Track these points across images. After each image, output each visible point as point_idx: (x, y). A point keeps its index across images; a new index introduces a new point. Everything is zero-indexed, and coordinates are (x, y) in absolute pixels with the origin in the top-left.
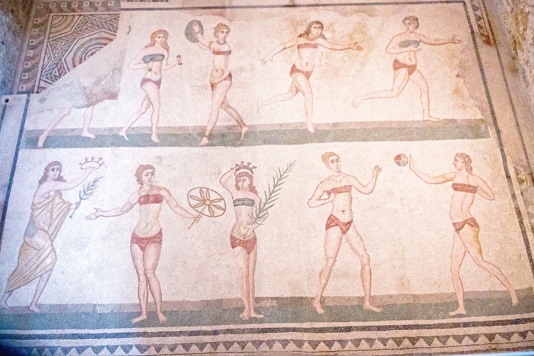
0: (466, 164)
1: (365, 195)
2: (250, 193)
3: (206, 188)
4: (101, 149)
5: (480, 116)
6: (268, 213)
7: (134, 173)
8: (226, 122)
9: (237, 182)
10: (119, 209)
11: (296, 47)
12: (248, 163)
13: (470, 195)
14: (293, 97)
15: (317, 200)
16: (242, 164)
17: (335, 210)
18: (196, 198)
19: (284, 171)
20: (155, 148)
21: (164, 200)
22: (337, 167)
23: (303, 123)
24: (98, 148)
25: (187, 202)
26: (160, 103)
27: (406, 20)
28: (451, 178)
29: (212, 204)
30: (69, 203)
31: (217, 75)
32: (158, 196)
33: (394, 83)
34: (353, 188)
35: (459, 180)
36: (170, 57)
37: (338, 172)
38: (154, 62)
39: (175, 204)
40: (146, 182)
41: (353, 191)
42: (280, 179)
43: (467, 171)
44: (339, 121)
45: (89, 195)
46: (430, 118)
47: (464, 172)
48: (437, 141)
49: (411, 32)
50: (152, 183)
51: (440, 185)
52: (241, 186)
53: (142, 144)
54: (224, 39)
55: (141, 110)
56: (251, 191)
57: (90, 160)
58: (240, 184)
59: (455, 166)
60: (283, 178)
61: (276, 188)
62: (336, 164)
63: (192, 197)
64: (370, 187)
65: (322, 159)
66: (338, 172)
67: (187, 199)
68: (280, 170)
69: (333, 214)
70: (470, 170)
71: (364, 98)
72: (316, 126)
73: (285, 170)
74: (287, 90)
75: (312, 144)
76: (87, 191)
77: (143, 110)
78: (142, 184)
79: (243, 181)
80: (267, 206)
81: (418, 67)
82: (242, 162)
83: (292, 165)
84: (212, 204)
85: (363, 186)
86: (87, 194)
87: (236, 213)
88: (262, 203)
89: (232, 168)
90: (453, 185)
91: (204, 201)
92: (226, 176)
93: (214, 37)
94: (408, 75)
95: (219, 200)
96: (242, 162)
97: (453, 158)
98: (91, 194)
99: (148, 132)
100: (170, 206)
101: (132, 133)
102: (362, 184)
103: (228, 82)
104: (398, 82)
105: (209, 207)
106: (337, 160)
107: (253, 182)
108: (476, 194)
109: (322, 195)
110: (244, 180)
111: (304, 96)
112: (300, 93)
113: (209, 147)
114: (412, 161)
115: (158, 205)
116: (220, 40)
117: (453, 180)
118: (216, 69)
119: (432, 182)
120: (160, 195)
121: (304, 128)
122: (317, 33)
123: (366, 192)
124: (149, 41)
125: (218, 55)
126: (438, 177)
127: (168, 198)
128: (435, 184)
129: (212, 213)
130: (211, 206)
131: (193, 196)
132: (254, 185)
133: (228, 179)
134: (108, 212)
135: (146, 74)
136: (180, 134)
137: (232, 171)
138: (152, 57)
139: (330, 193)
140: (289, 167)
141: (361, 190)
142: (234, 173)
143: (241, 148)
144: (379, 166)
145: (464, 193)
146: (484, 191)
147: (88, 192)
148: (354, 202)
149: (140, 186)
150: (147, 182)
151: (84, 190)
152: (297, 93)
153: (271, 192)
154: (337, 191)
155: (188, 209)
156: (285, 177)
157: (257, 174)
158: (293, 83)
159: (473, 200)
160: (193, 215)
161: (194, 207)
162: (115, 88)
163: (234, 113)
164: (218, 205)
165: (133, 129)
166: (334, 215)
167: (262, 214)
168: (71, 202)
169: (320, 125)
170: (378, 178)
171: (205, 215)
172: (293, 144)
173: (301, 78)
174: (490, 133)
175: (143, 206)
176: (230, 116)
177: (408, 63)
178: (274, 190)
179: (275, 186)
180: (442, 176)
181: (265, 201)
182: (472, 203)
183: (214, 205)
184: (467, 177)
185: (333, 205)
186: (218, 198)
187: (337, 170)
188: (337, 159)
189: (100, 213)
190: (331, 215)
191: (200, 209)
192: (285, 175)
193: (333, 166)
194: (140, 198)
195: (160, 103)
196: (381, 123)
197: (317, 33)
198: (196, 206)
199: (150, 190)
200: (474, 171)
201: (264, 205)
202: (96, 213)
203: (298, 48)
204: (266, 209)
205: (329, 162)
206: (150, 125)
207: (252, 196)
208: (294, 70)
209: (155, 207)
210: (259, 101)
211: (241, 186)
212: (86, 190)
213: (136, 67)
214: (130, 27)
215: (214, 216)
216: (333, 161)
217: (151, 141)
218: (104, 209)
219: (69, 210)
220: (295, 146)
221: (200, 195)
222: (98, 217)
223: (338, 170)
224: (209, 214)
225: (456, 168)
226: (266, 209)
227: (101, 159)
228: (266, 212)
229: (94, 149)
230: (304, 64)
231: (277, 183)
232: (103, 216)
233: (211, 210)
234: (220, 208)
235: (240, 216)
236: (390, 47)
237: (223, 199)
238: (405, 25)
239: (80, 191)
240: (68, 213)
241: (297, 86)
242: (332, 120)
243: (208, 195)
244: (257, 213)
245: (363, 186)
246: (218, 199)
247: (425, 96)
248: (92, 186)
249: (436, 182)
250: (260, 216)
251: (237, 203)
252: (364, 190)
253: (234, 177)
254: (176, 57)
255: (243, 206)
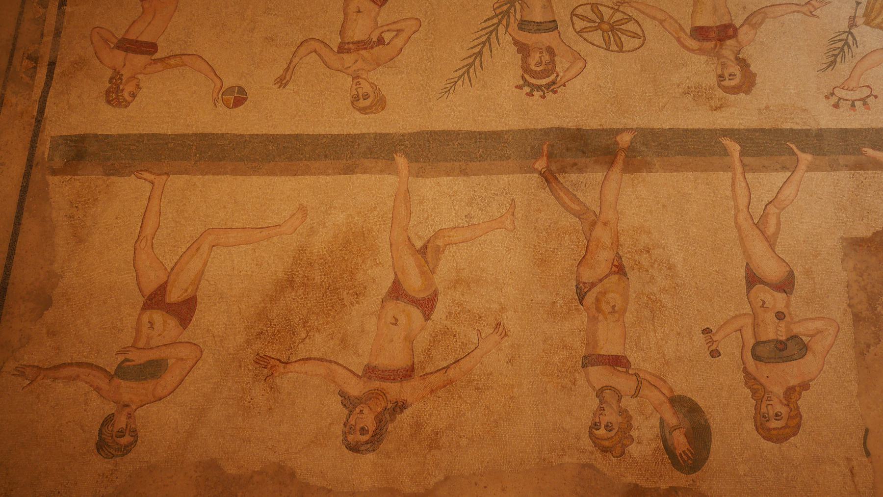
0: (118, 87)
1: (317, 38)
2: (527, 42)
3: (612, 51)
4: (843, 127)
5: (53, 180)
6: (494, 10)
7: (758, 80)
8: (583, 181)
9: (553, 62)
10: (772, 15)
11: (418, 373)
12: (533, 95)
13: (132, 36)
14: (437, 235)
15: (402, 30)
16: (544, 93)
17: (373, 14)
18: (629, 34)
19: (462, 79)
20: (727, 126)
21: (688, 31)
22: (358, 86)
23: (417, 176)
24: (848, 127)
25: (644, 28)
26: (738, 227)
27: (126, 446)
28: (154, 64)
29: (597, 24)
30: (871, 26)
31: (614, 297)
32: (701, 38)
33: (205, 264)
34: (336, 50)
35: (140, 60)
36: (737, 353)
37: (358, 77)
38: (775, 338)
39: (666, 24)
40: (730, 63)
41: (335, 44)
42: (470, 65)
43: (122, 75)
44: (342, 177)
45: (836, 39)
46: (154, 180)
47: (126, 73)
48: (155, 132)
49: (127, 406)
50: (718, 60)
51: (178, 52)
52: (544, 54)
53: (757, 135)
54: (604, 405)
55: (777, 211)
56: (525, 44)
57: (857, 103)
58: (546, 57)
59: (139, 85)
60: (463, 67)
61: (478, 50)
62: (360, 92)
63: (635, 35)
64: (302, 51)
65: (385, 102)
66: (358, 77)
67: (646, 33)
68: (470, 81)
69: (377, 8)
70: (116, 79)
71: (278, 229)
72: (391, 168)
73: (460, 82)
74: (446, 252)
75: (401, 132)
76: (843, 46)
77: (772, 209)
78: (737, 59)
79: (541, 61)
80: (495, 20)
81: (141, 300)
82: (543, 97)
83: (446, 92)
84: (597, 24)
85: (315, 51)
86: (841, 40)
87: (553, 11)
88: (505, 25)
89: (564, 85)
90: (156, 51)
91: (612, 28)
92: (573, 72)
93: (631, 413)
94: (169, 284)
95: (585, 30)
96: (543, 97)
97: (137, 98)
98: (833, 41)
99: (747, 160)
100: (676, 22)
101: (783, 158)
102: (317, 57)
103: (588, 275)
104: (195, 265)
105: (602, 19)
106: (356, 98)
107: (522, 61)
108: (120, 34)
109: (393, 38)
110: (539, 64)
111: (409, 239)
112: (419, 244)
113: (615, 126)
114: (215, 95)
115: (700, 23)
116: (614, 406)
117: (152, 60)
118: (616, 315)
119: (190, 57)
120: (699, 40)
121: (415, 164)
122: (361, 411)
123: (313, 42)
124: (805, 402)
125: (615, 354)
126: (176, 66)
127: (682, 34)
128: (186, 54)
129: (595, 10)
130: (598, 21)
131: (634, 37)
132: (520, 56)
133: (571, 65)
134: (789, 11)
135: (788, 306)
136: (679, 154)
137: (563, 80)
138: (785, 353)
139: (378, 41)
140: (451, 87)
141: (322, 46)
142: (559, 78)
143: (548, 125)
144: (279, 87)
145: (140, 39)
146: (106, 41)
147: (840, 44)
148: (338, 26)
149: (741, 56)
150: (730, 63)
151: (849, 47)
152: (425, 247)
153: (487, 44)
154: (365, 45)
155: (642, 16)
156: (460, 69)
157: (514, 75)
158: (433, 271)
159: (130, 27)
160: (632, 7)
161: (630, 19)
162: (854, 268)
163: (567, 200)
164: (585, 23)
165: (784, 168)
166: (376, 6)
167: (505, 8)
168: (868, 28)
169: (381, 172)
170: (285, 66)
171: (608, 7)
172: (440, 131)
173: (414, 283)
174: (48, 145)
175: (726, 21)
176: (575, 193)
177: (158, 316)
178: (483, 47)
179: (480, 53)
180: (170, 67)
181: (499, 28)
182: (132, 24)
183: (595, 22)
184: (125, 65)
185: (376, 22)
186: (586, 34)
187: (360, 80)
188: (357, 101)
189: (805, 9)
190: (380, 6)
191: (618, 16)
192: (461, 72)
193: (366, 88)
194: (735, 35)
195: (738, 227)
196: (255, 171)
197: (361, 411)
198: (626, 21)
199: (721, 48)
200: (109, 73)
201: (500, 22)
202: (812, 9)
203: (412, 369)
204: (496, 15)
205: (372, 95)
206: (749, 176)
207: (524, 37)
208: (427, 305)
209: (705, 20)
210: (510, 227)
211: (544, 54)
212: (846, 48)
213: (819, 324)
214: (868, 454)
215: (592, 5)
216: (366, 96)
217: (738, 141)
218: (798, 16)
219: (866, 15)
220: (438, 127)
221: (623, 39)
222: (806, 4)
223: (358, 80)
224: (601, 8)
225: (139, 82)
226: (496, 15)
227: (836, 106)
228: (498, 11)
229: (856, 125)
230: (402, 319)
231: (476, 58)
232: (798, 5)
233: (598, 14)
234: (583, 18)
235: (545, 5)
236: (190, 363)
237: (578, 33)
238: (135, 431)
239: (857, 46)
240: (866, 9)
241: (423, 262)
242: (359, 179)
243: (607, 39)
244: (513, 9)
245: (315, 51)
246: (586, 32)
247: (148, 231)
248: (836, 56)
249: (183, 57)
250: (509, 5)
251: (551, 25)
252: (314, 45)
253: (558, 69)
254: (721, 352)
255: (539, 21)
